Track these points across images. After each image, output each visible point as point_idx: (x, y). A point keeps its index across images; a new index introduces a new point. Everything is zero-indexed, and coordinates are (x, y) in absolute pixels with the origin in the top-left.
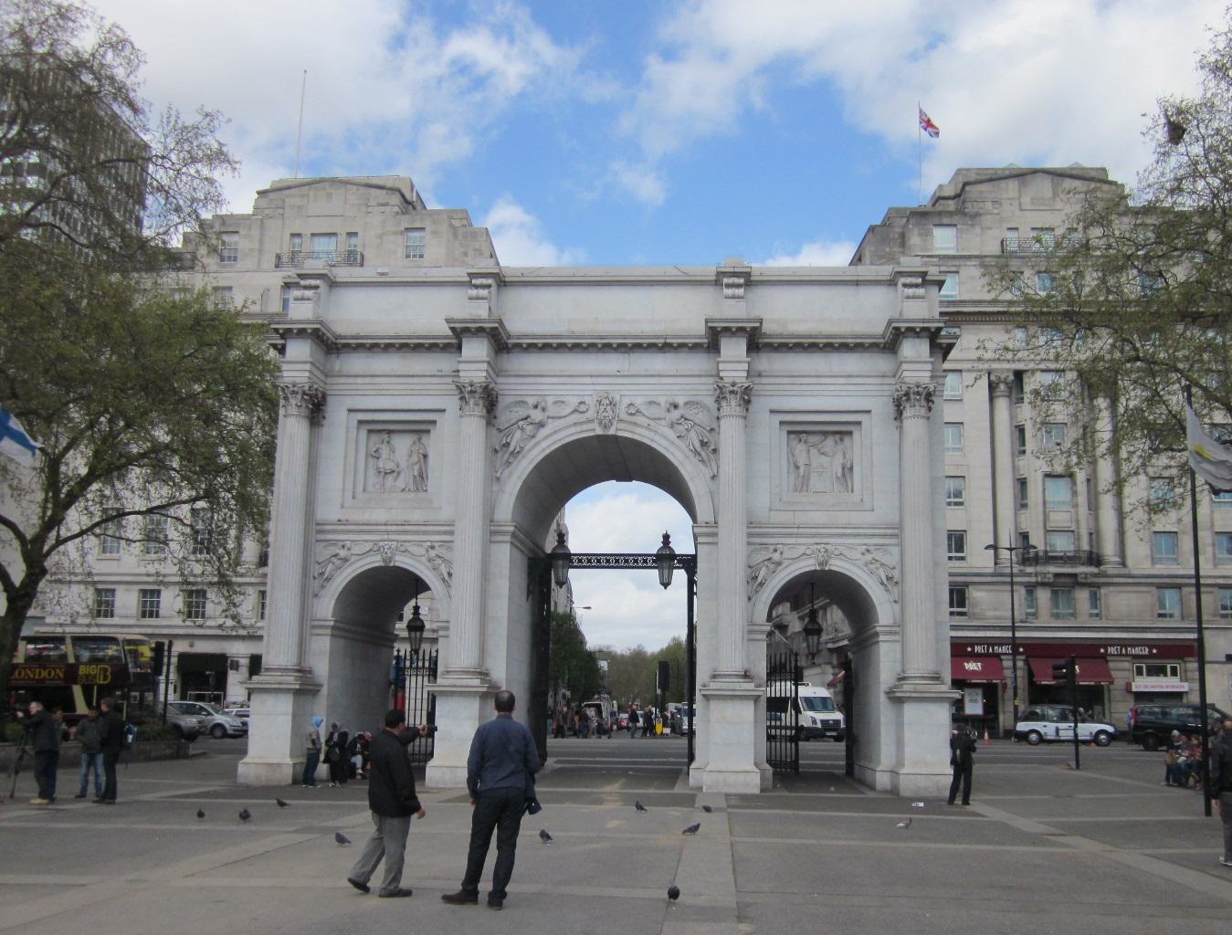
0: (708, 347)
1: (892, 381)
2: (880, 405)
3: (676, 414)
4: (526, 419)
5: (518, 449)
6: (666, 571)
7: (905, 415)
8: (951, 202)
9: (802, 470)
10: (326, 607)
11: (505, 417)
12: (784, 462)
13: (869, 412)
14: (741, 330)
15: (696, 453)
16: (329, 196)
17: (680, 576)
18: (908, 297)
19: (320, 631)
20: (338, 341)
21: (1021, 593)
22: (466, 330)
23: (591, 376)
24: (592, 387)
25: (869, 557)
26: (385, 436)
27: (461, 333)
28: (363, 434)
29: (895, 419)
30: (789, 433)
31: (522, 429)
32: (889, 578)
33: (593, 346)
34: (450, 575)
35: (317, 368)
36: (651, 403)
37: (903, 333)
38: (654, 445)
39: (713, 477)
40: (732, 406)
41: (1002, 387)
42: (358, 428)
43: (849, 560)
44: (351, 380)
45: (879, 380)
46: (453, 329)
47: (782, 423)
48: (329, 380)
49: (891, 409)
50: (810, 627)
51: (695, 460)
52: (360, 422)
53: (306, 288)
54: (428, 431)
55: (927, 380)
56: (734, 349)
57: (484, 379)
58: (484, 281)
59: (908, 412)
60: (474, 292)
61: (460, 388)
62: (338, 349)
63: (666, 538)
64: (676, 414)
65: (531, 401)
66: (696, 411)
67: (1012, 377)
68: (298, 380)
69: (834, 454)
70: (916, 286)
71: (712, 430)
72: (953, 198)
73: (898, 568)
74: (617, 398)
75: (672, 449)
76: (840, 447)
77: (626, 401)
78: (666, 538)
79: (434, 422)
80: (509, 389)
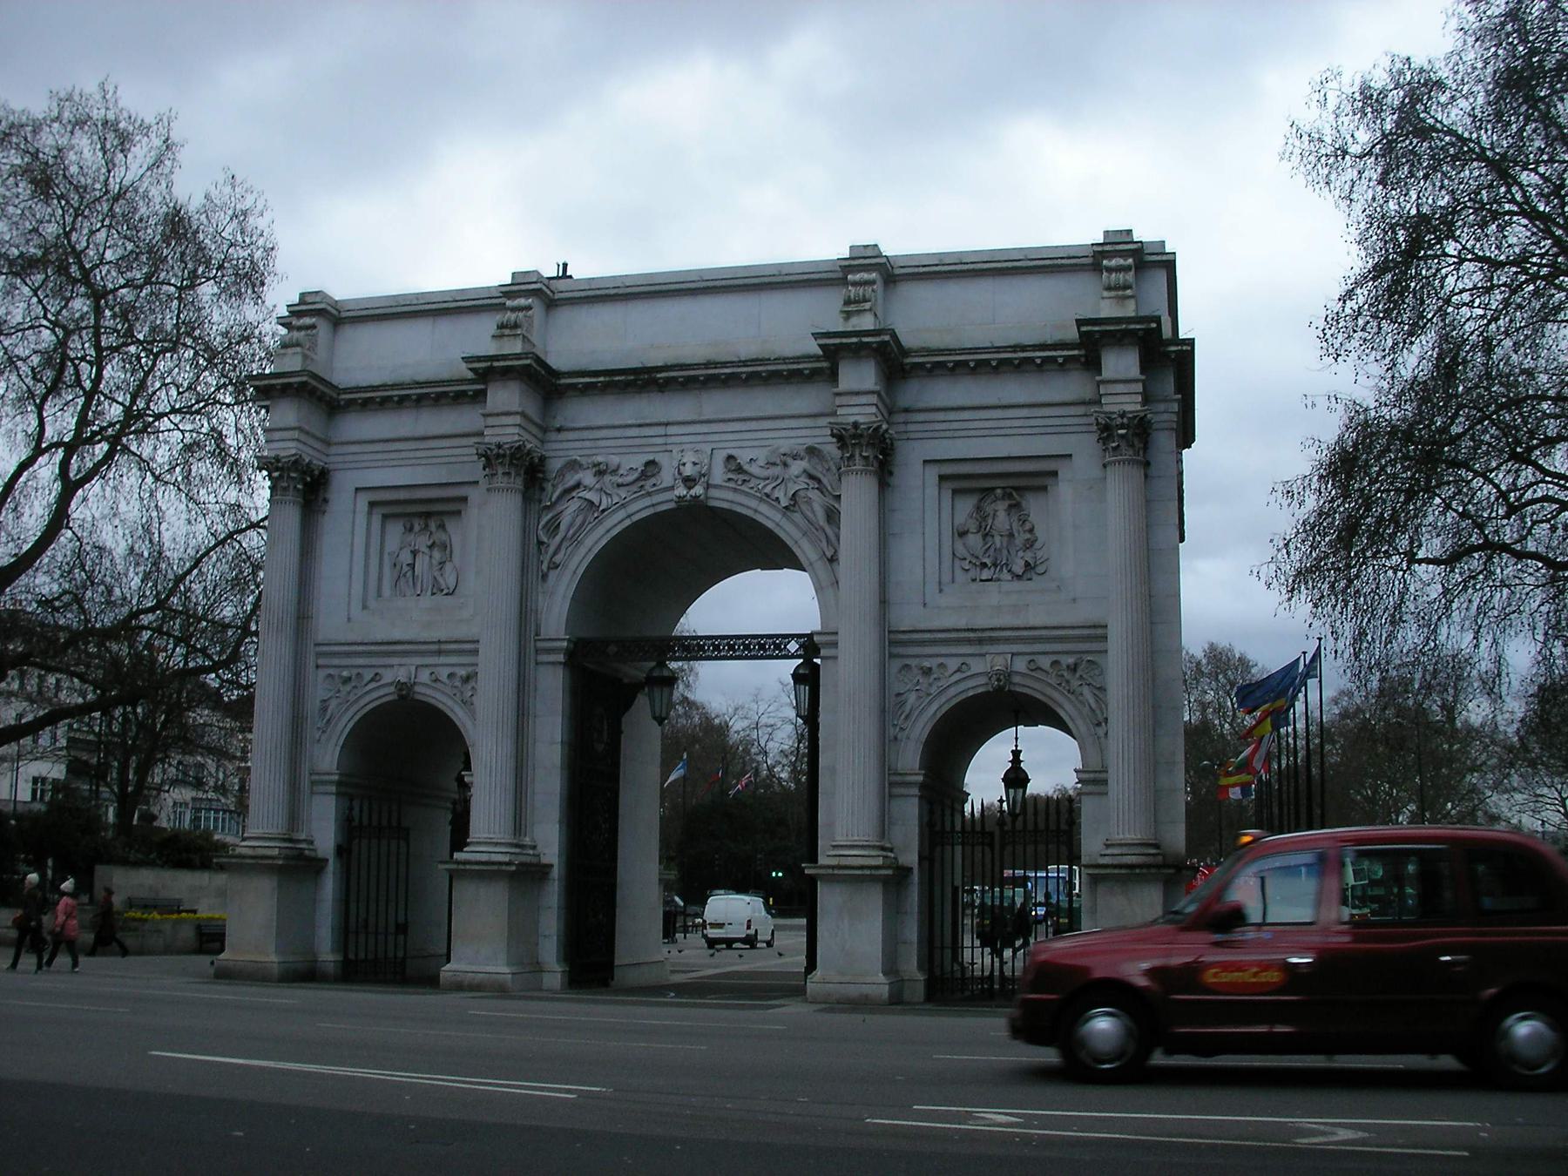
10: (327, 756)
19: (321, 788)
27: (488, 372)
28: (377, 520)
35: (307, 433)
42: (370, 513)
45: (1081, 410)
47: (942, 478)
48: (333, 450)
54: (459, 513)
56: (860, 376)
79: (464, 499)
80: (559, 451)
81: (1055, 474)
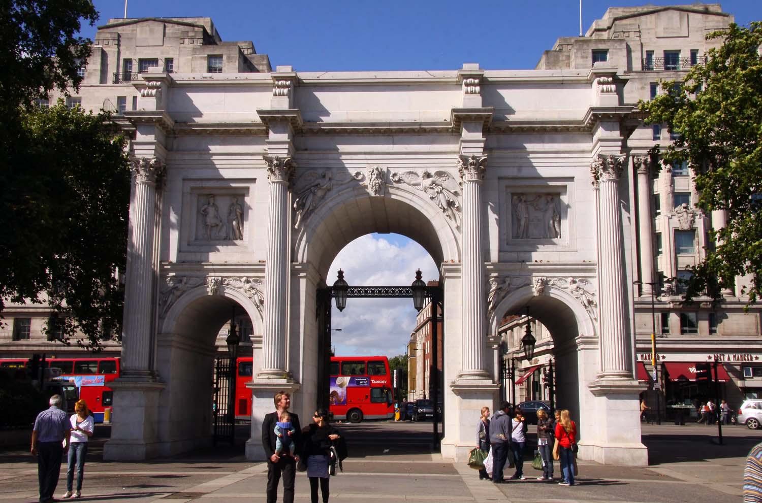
0: (452, 131)
1: (590, 155)
2: (583, 175)
4: (317, 185)
5: (311, 208)
6: (419, 300)
7: (601, 179)
8: (603, 33)
9: (523, 223)
11: (301, 184)
12: (510, 217)
13: (571, 179)
14: (478, 118)
17: (427, 303)
18: (603, 91)
20: (175, 128)
21: (659, 315)
22: (274, 119)
23: (365, 154)
24: (365, 162)
25: (575, 286)
26: (212, 201)
29: (593, 183)
30: (513, 194)
31: (314, 194)
32: (590, 302)
33: (367, 131)
34: (262, 302)
36: (410, 173)
37: (599, 118)
38: (412, 204)
39: (458, 228)
40: (471, 175)
41: (643, 166)
43: (560, 289)
44: (186, 157)
46: (261, 118)
47: (507, 187)
50: (526, 339)
51: (443, 215)
52: (192, 189)
53: (150, 88)
55: (618, 153)
57: (286, 156)
58: (284, 82)
59: (605, 177)
60: (278, 91)
61: (269, 160)
62: (174, 134)
63: (419, 274)
64: (428, 181)
65: (320, 172)
66: (444, 179)
68: (146, 157)
69: (546, 211)
70: (608, 83)
71: (456, 192)
72: (604, 30)
73: (597, 294)
74: (385, 170)
75: (426, 207)
76: (551, 206)
77: (393, 172)
78: (419, 274)
81: (565, 187)
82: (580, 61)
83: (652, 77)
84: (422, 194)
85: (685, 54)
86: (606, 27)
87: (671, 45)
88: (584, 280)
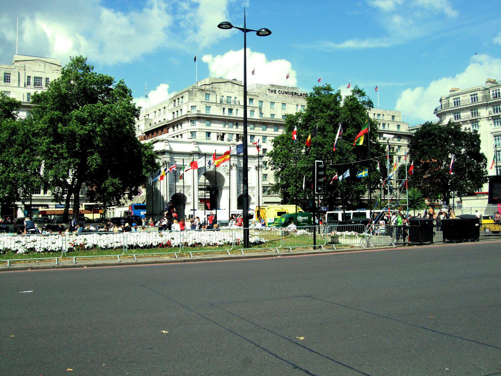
3: (223, 168)
15: (226, 174)
16: (40, 65)
41: (220, 137)
49: (255, 168)
64: (223, 168)
67: (222, 135)
82: (201, 97)
83: (224, 106)
84: (222, 170)
85: (233, 99)
86: (208, 84)
87: (229, 94)
88: (253, 190)
